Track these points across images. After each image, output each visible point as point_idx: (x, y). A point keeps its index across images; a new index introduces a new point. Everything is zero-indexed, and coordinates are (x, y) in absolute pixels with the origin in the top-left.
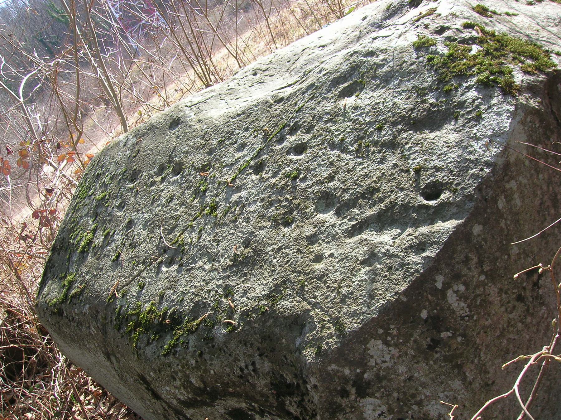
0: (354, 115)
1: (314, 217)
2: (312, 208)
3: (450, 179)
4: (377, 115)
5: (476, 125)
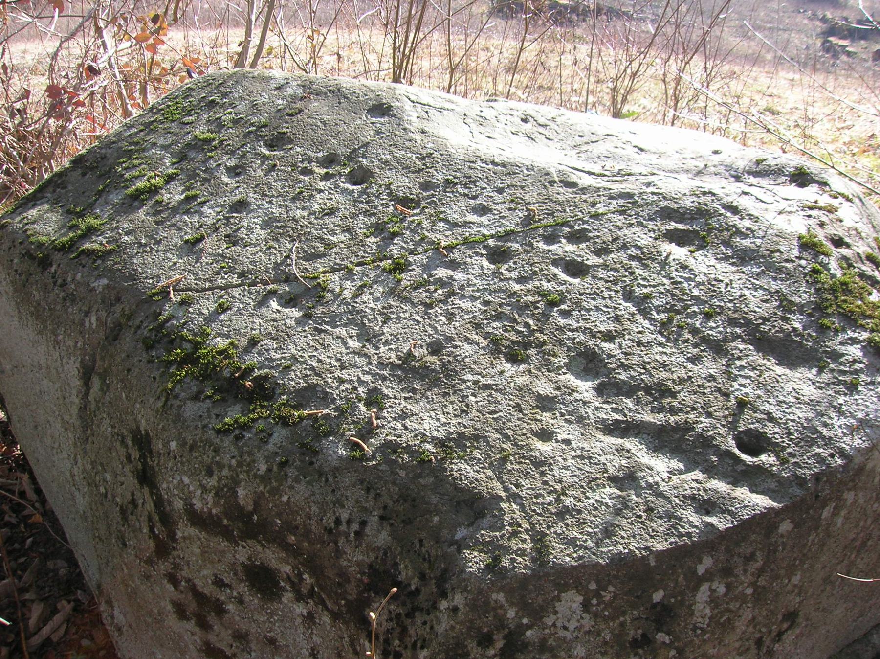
0: (677, 273)
1: (560, 374)
2: (562, 360)
3: (783, 442)
4: (712, 296)
5: (845, 395)
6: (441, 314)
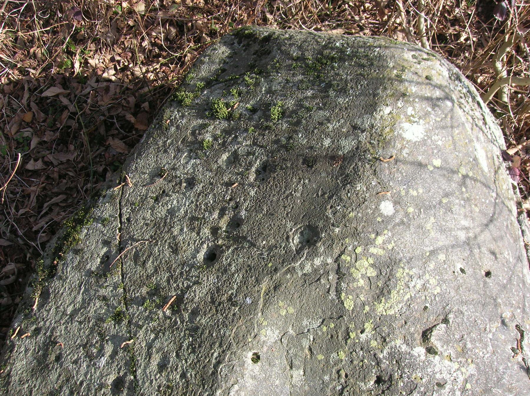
6: (78, 355)
